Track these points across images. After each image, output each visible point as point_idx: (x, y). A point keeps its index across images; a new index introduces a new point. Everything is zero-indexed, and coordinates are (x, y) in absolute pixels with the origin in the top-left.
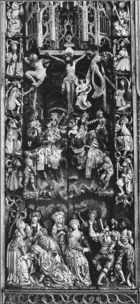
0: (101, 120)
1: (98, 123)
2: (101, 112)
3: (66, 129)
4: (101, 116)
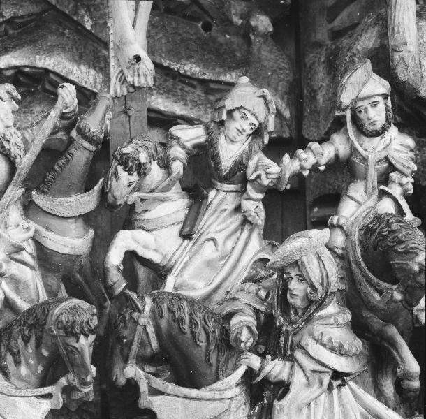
0: (372, 149)
1: (345, 169)
2: (379, 86)
3: (87, 219)
4: (377, 115)
